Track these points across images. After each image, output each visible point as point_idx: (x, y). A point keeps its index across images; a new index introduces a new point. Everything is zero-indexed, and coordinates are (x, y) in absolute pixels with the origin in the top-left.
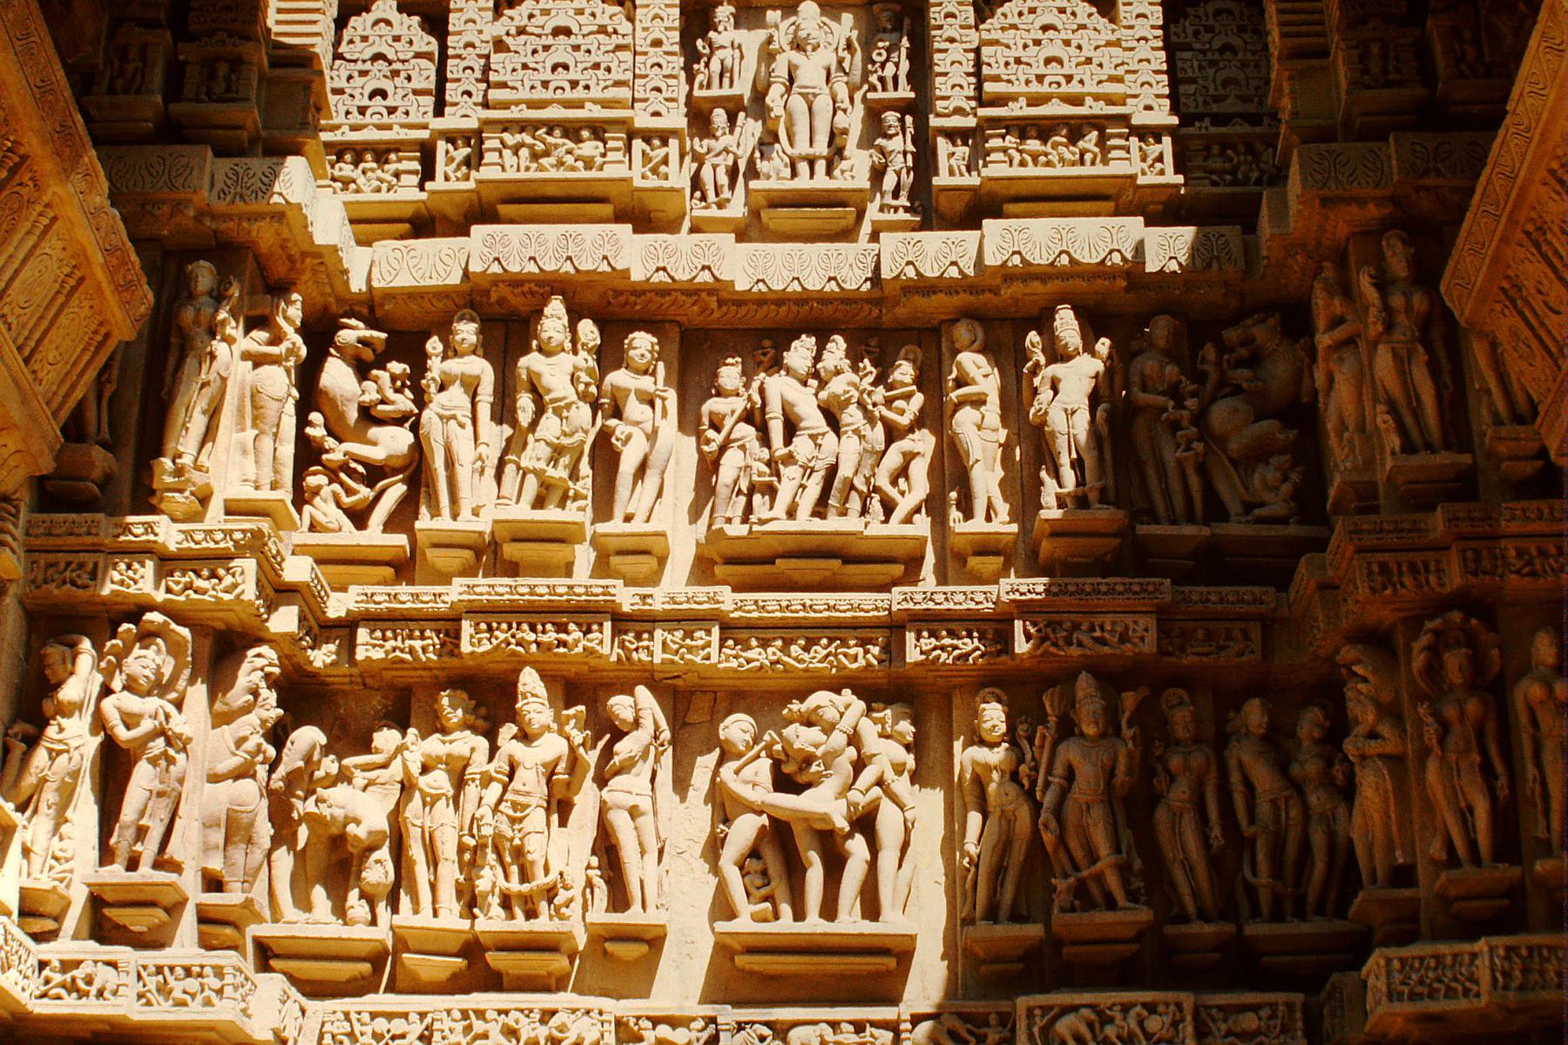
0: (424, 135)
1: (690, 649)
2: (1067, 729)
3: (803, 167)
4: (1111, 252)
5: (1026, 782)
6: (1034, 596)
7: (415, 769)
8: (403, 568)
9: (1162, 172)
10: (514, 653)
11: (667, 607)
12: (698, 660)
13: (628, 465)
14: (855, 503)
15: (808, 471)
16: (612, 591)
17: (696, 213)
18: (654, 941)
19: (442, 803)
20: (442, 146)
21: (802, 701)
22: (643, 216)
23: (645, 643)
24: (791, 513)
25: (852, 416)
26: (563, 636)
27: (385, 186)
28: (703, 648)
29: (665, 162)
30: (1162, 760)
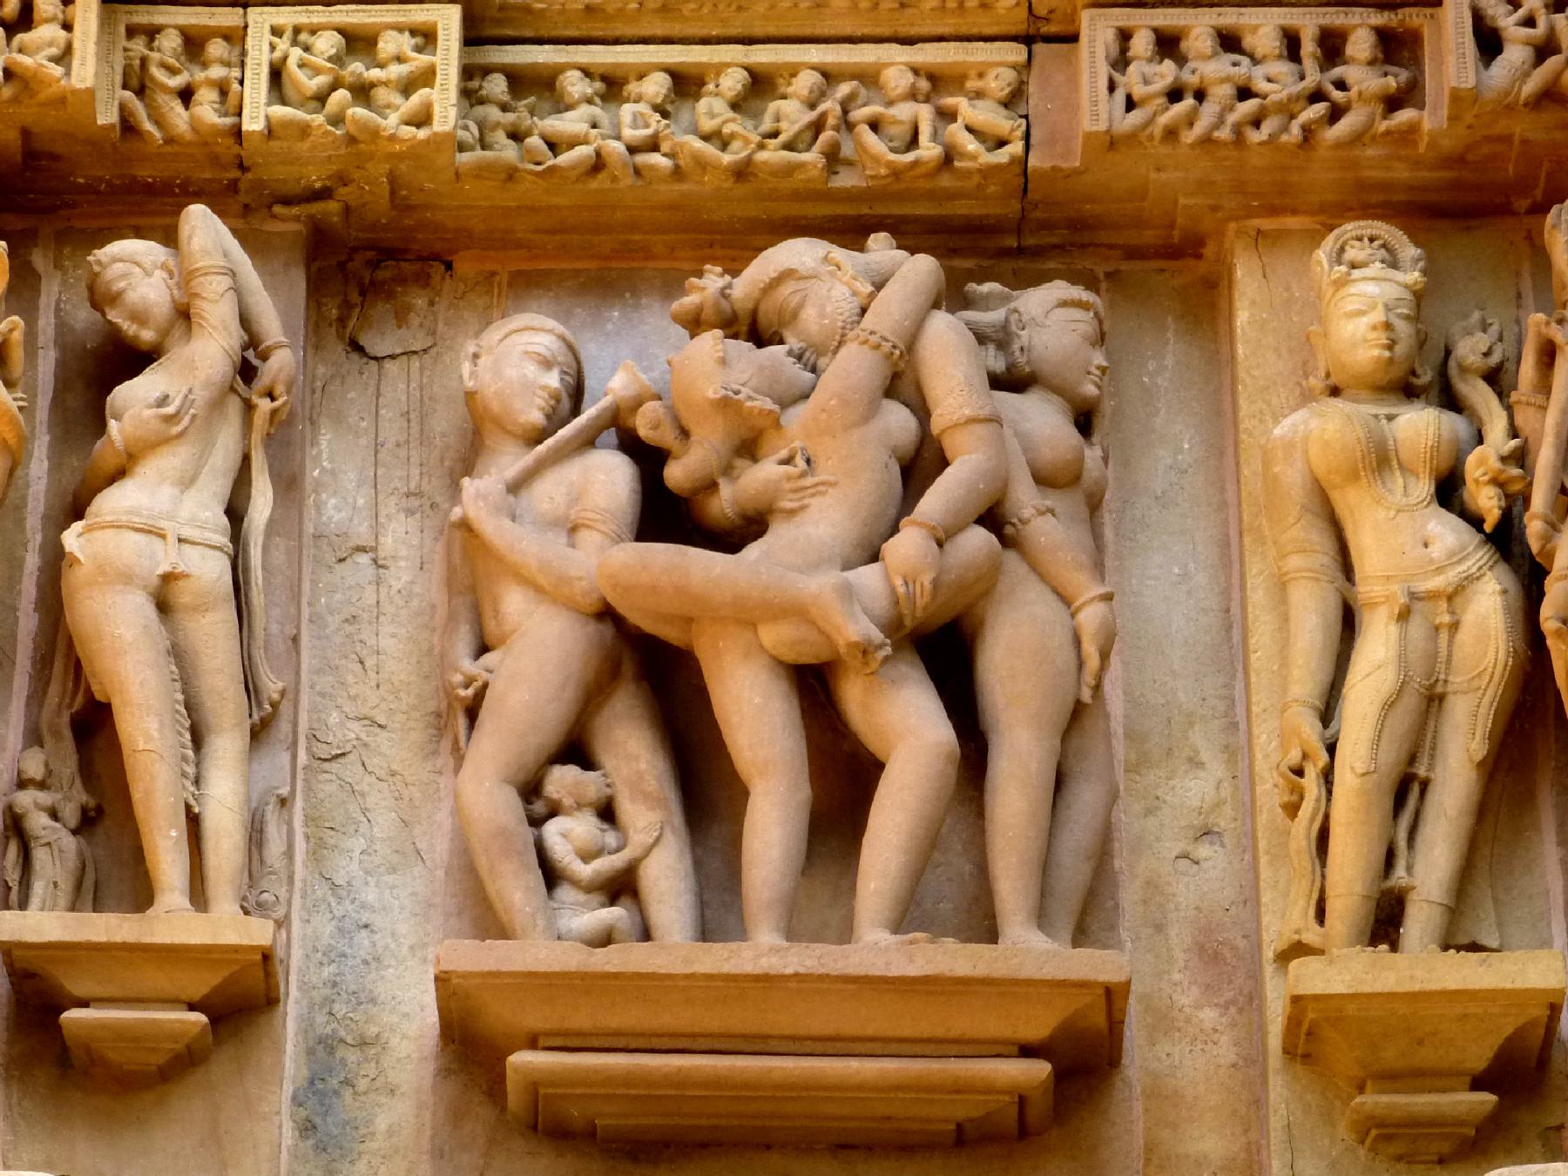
1: (362, 92)
5: (1488, 502)
12: (391, 122)
18: (240, 1002)
23: (216, 72)
28: (407, 87)
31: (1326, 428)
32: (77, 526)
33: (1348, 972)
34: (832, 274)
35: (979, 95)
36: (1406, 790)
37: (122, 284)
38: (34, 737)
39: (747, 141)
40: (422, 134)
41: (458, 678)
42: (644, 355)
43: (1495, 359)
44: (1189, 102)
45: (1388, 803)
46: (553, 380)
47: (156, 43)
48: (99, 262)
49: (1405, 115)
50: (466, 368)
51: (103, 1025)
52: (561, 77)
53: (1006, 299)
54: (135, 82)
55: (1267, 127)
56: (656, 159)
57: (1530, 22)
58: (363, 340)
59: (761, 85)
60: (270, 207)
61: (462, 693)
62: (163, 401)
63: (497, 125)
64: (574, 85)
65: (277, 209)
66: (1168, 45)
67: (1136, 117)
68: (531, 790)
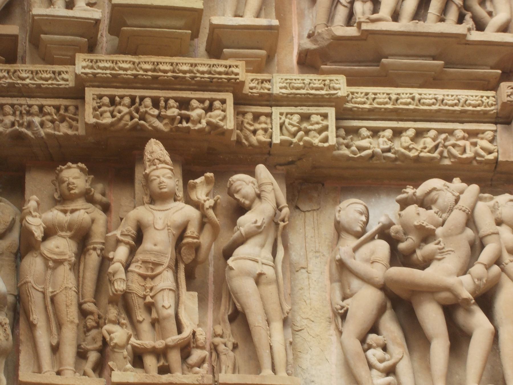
7: (38, 234)
11: (284, 91)
16: (235, 70)
21: (416, 186)
23: (264, 126)
24: (396, 16)
28: (320, 132)
32: (231, 259)
34: (446, 189)
35: (482, 139)
37: (240, 187)
38: (216, 321)
39: (417, 150)
40: (326, 145)
41: (339, 307)
47: (246, 117)
48: (233, 181)
52: (361, 130)
53: (491, 199)
54: (239, 128)
56: (390, 155)
58: (300, 206)
59: (420, 134)
60: (275, 166)
61: (340, 311)
62: (256, 222)
63: (342, 144)
64: (364, 132)
65: (278, 167)
68: (363, 341)
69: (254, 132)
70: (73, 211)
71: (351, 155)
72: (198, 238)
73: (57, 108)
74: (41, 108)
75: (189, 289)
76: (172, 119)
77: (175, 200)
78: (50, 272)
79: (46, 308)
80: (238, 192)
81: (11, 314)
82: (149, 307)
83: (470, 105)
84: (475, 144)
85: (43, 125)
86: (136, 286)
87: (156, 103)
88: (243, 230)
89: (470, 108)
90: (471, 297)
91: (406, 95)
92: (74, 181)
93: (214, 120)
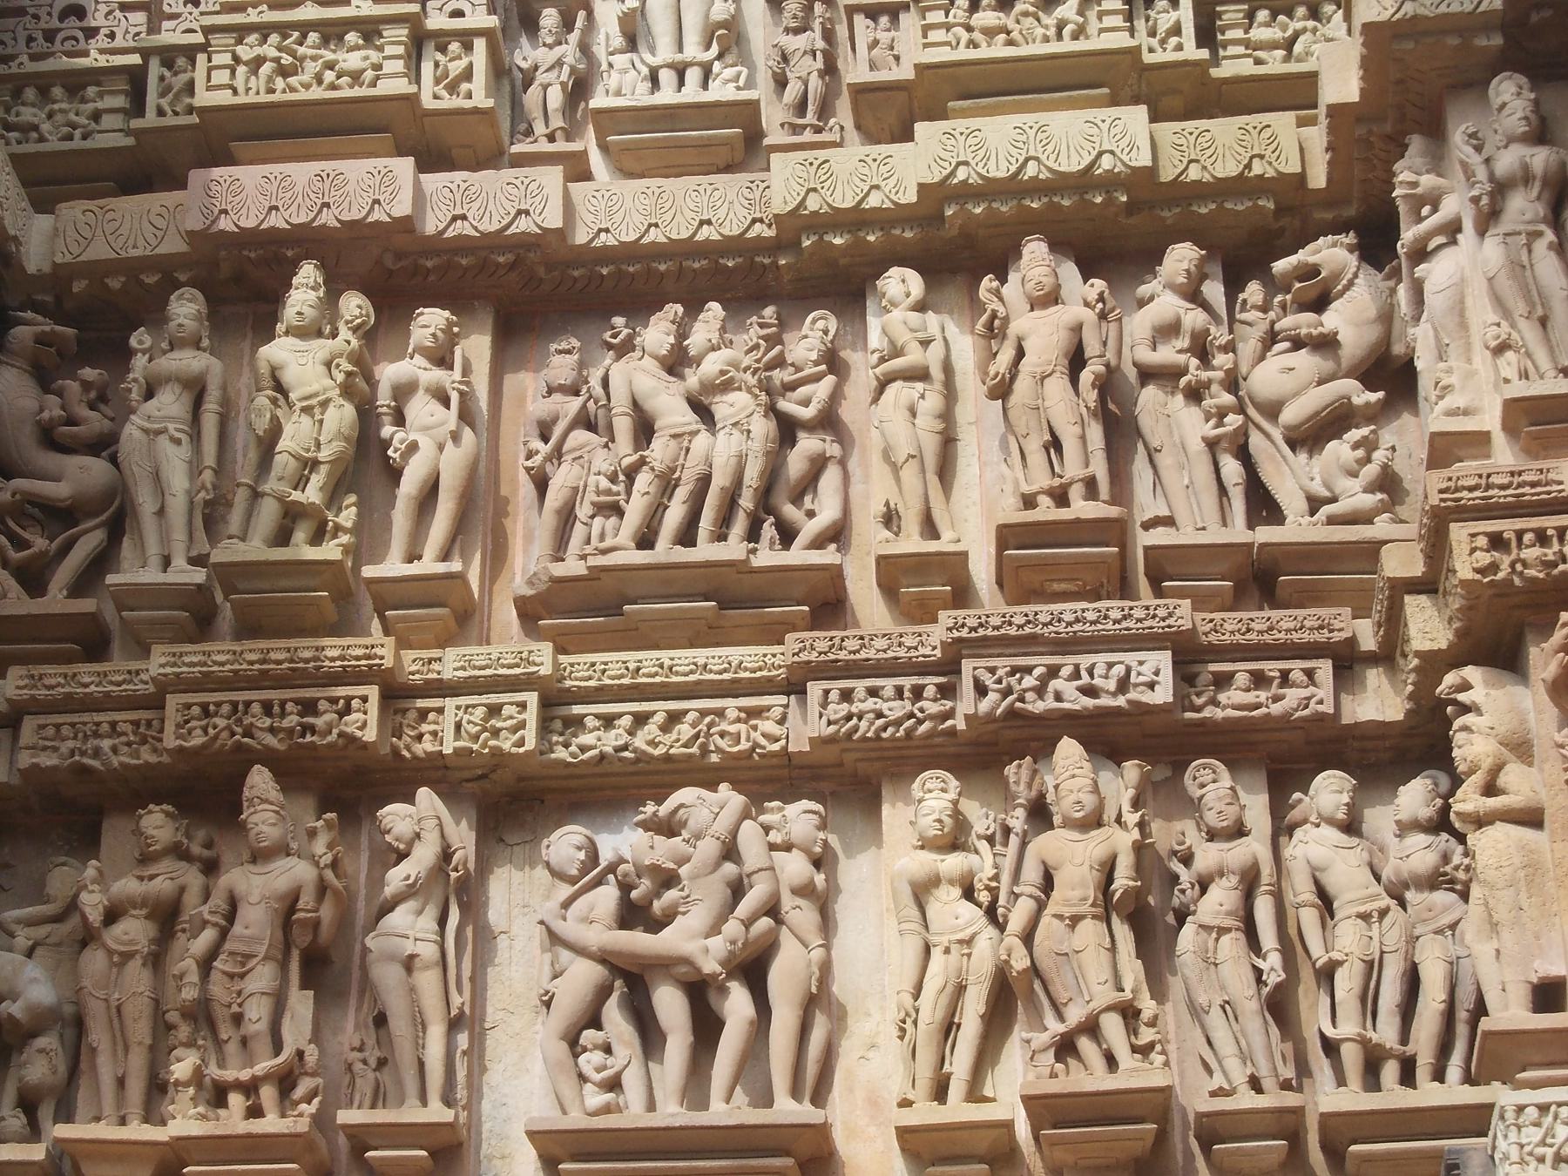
0: (135, 59)
2: (1040, 814)
3: (666, 76)
4: (1100, 154)
6: (989, 632)
8: (92, 642)
9: (1179, 47)
10: (239, 747)
11: (461, 674)
12: (507, 745)
13: (410, 484)
14: (739, 526)
15: (667, 484)
16: (378, 651)
17: (515, 149)
19: (135, 965)
20: (155, 69)
22: (436, 145)
23: (433, 727)
24: (646, 540)
25: (727, 407)
26: (311, 720)
27: (78, 133)
29: (467, 75)
30: (1187, 860)
31: (928, 861)
33: (927, 1113)
36: (949, 1028)
38: (357, 1027)
42: (625, 842)
43: (989, 832)
44: (855, 720)
45: (941, 1037)
46: (582, 855)
49: (949, 723)
50: (544, 852)
51: (382, 1159)
53: (781, 809)
55: (890, 730)
56: (626, 754)
57: (999, 681)
59: (674, 718)
62: (408, 878)
64: (590, 722)
66: (846, 696)
67: (833, 728)
69: (420, 737)
70: (152, 878)
71: (570, 760)
72: (316, 911)
73: (136, 724)
74: (113, 724)
75: (304, 986)
76: (290, 732)
77: (288, 855)
78: (115, 970)
79: (111, 1021)
80: (388, 832)
81: (70, 1033)
82: (238, 1019)
83: (746, 669)
84: (755, 728)
85: (115, 753)
86: (218, 989)
87: (267, 708)
88: (389, 891)
89: (747, 675)
90: (719, 969)
91: (649, 663)
92: (154, 832)
93: (348, 730)
